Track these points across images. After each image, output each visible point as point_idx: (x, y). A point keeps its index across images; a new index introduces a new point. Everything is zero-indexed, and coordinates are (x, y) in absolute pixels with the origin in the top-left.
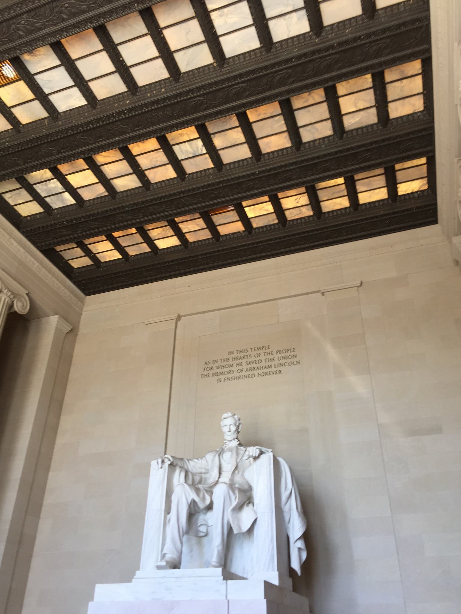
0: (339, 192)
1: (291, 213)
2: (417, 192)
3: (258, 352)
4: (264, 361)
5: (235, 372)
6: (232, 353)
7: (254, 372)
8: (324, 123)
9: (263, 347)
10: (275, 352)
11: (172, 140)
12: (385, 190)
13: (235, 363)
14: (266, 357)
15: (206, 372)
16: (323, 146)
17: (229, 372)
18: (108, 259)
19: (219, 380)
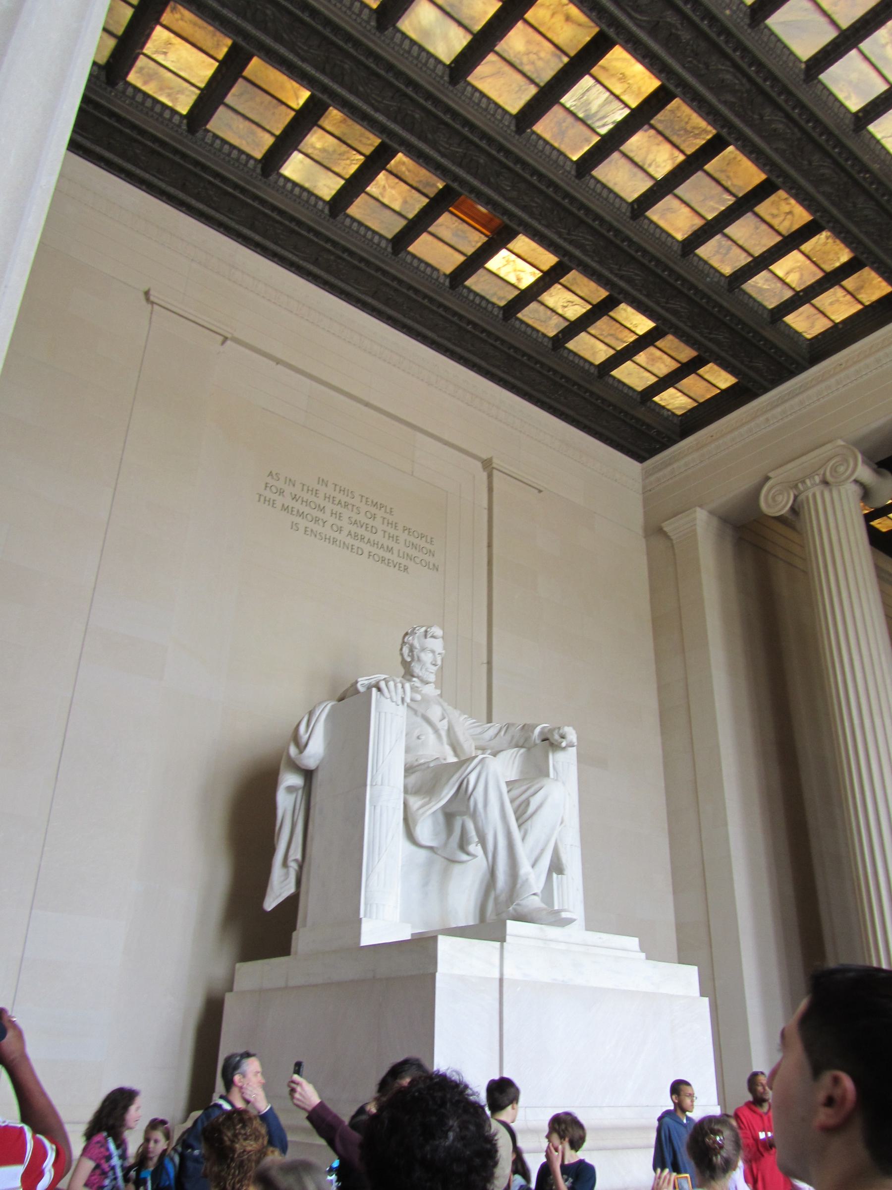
0: (617, 339)
1: (536, 311)
2: (668, 410)
3: (374, 510)
4: (380, 533)
5: (328, 525)
6: (323, 482)
7: (362, 545)
8: (744, 255)
9: (382, 506)
10: (400, 527)
11: (604, 68)
12: (653, 380)
13: (329, 506)
14: (385, 527)
15: (268, 494)
16: (708, 279)
17: (316, 520)
18: (149, 89)
19: (295, 526)
